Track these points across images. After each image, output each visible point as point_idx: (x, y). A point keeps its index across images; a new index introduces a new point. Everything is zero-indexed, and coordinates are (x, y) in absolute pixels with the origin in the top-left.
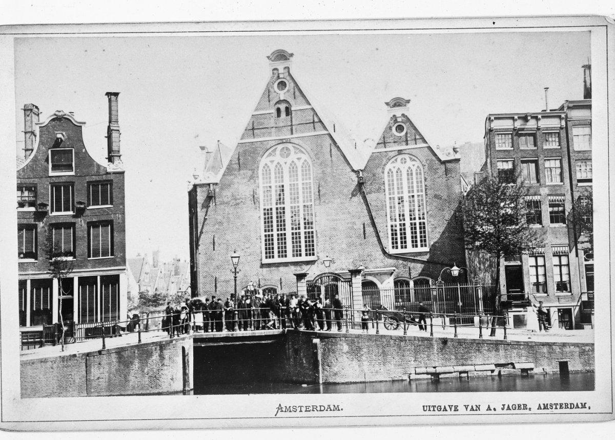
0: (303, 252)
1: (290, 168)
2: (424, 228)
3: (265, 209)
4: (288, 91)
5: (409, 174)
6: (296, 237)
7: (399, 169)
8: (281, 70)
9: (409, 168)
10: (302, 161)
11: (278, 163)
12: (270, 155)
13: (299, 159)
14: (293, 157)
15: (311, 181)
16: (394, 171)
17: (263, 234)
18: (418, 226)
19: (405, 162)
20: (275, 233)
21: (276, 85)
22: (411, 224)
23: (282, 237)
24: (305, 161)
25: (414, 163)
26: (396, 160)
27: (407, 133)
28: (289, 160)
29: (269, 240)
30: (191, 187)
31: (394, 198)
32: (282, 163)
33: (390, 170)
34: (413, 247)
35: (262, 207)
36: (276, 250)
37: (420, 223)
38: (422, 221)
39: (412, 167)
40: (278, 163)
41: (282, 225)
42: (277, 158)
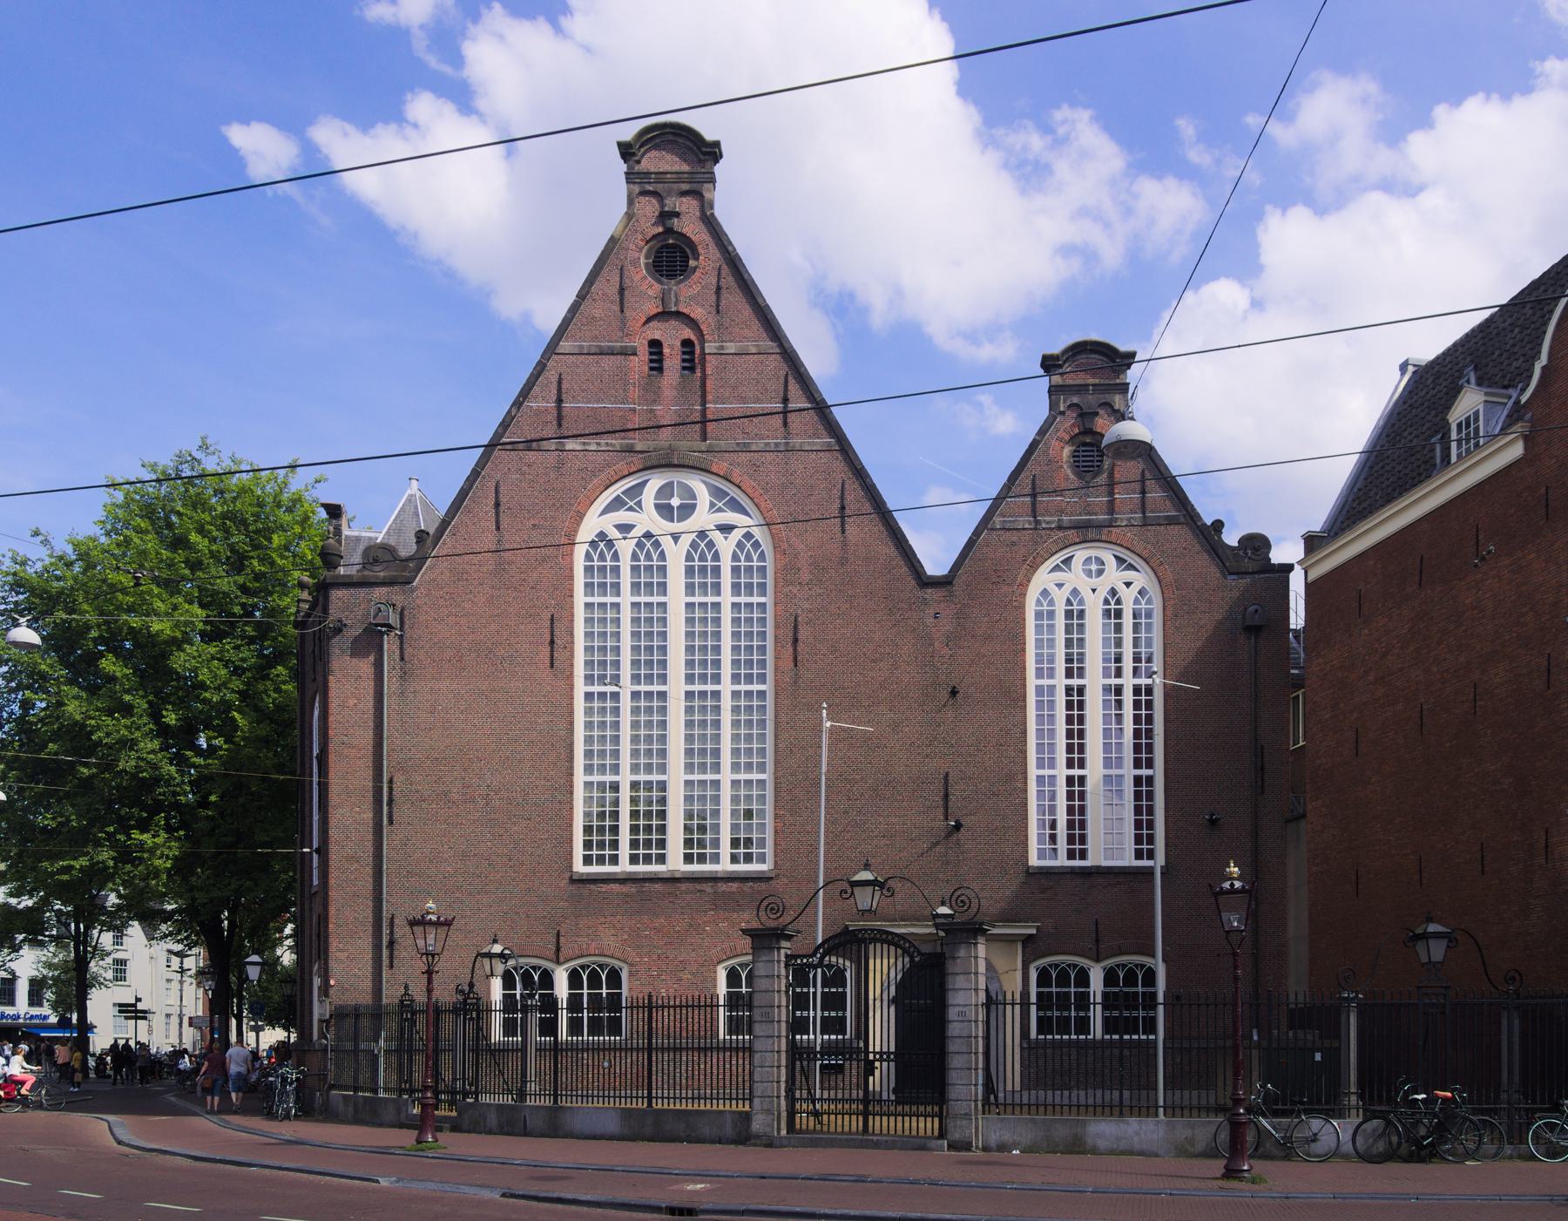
1: (689, 557)
7: (1075, 592)
9: (1113, 592)
10: (737, 535)
11: (648, 535)
12: (617, 504)
13: (726, 529)
19: (1100, 572)
25: (1130, 575)
26: (1067, 561)
33: (1045, 593)
39: (1121, 588)
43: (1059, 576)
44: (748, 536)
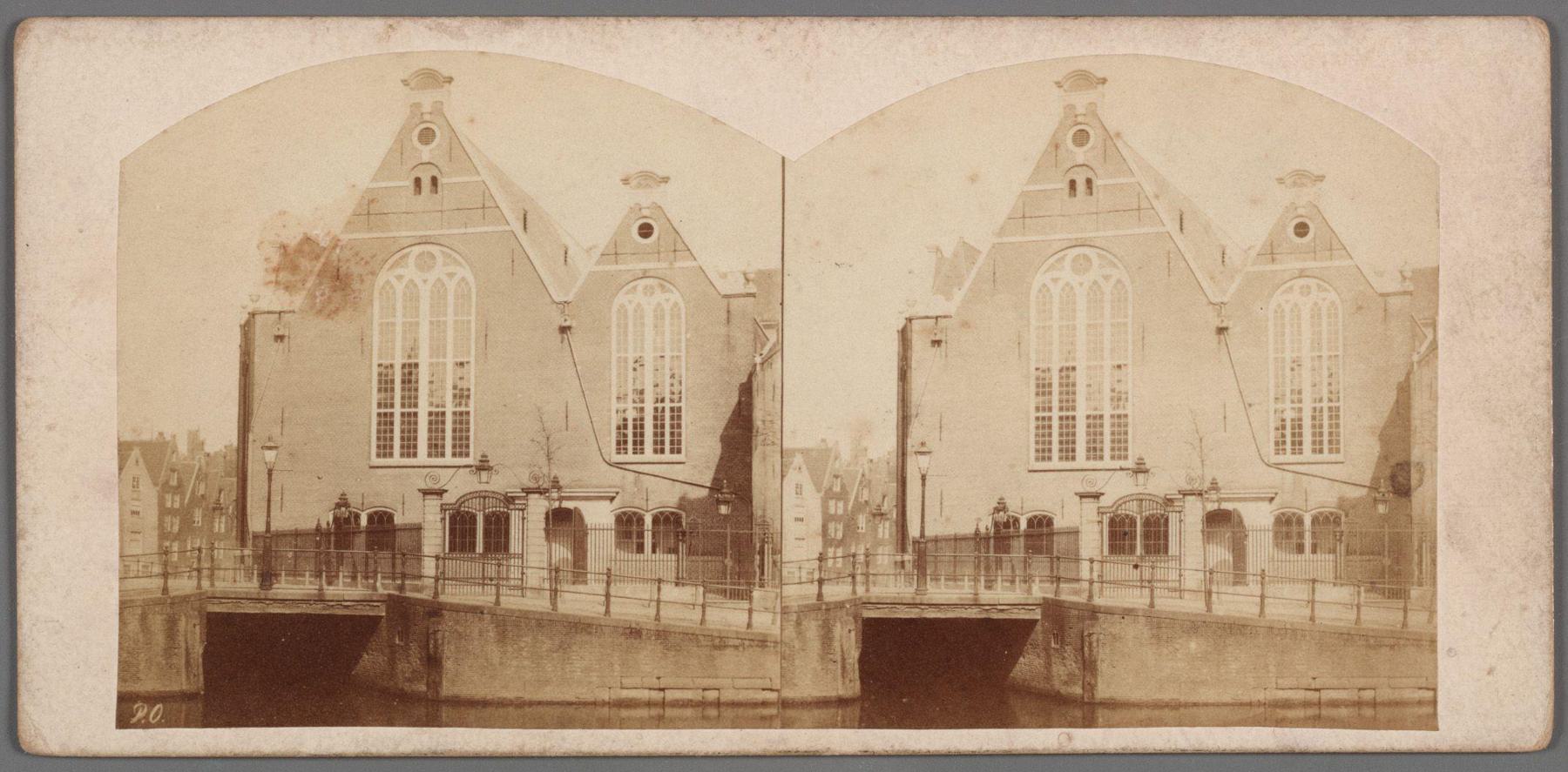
0: (448, 450)
2: (679, 417)
3: (380, 365)
4: (439, 145)
5: (659, 315)
6: (437, 419)
8: (427, 108)
14: (438, 272)
15: (473, 318)
16: (630, 308)
17: (375, 410)
18: (667, 414)
20: (397, 410)
21: (416, 132)
22: (656, 409)
23: (410, 419)
24: (463, 279)
26: (635, 288)
27: (659, 239)
28: (432, 276)
29: (386, 420)
30: (245, 317)
31: (626, 360)
32: (418, 282)
33: (622, 306)
34: (655, 451)
35: (375, 362)
36: (397, 443)
37: (672, 409)
38: (676, 405)
40: (411, 281)
41: (411, 399)
42: (410, 271)
43: (630, 296)
44: (463, 279)
